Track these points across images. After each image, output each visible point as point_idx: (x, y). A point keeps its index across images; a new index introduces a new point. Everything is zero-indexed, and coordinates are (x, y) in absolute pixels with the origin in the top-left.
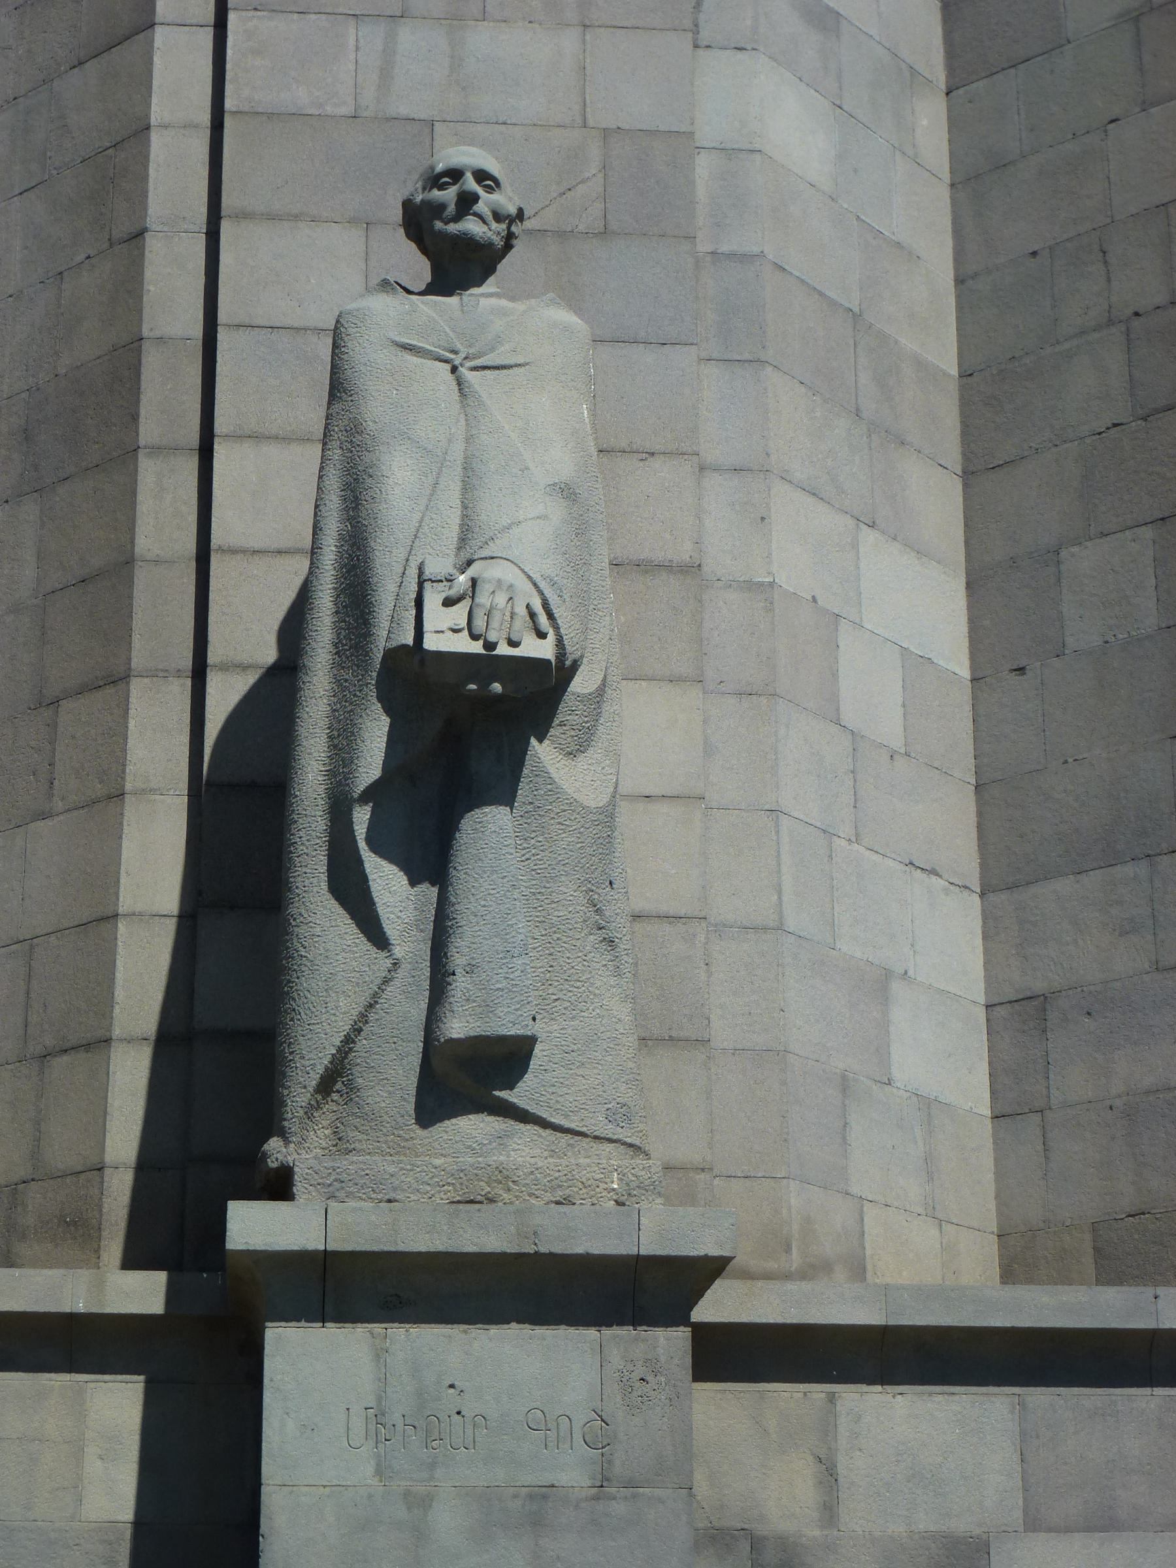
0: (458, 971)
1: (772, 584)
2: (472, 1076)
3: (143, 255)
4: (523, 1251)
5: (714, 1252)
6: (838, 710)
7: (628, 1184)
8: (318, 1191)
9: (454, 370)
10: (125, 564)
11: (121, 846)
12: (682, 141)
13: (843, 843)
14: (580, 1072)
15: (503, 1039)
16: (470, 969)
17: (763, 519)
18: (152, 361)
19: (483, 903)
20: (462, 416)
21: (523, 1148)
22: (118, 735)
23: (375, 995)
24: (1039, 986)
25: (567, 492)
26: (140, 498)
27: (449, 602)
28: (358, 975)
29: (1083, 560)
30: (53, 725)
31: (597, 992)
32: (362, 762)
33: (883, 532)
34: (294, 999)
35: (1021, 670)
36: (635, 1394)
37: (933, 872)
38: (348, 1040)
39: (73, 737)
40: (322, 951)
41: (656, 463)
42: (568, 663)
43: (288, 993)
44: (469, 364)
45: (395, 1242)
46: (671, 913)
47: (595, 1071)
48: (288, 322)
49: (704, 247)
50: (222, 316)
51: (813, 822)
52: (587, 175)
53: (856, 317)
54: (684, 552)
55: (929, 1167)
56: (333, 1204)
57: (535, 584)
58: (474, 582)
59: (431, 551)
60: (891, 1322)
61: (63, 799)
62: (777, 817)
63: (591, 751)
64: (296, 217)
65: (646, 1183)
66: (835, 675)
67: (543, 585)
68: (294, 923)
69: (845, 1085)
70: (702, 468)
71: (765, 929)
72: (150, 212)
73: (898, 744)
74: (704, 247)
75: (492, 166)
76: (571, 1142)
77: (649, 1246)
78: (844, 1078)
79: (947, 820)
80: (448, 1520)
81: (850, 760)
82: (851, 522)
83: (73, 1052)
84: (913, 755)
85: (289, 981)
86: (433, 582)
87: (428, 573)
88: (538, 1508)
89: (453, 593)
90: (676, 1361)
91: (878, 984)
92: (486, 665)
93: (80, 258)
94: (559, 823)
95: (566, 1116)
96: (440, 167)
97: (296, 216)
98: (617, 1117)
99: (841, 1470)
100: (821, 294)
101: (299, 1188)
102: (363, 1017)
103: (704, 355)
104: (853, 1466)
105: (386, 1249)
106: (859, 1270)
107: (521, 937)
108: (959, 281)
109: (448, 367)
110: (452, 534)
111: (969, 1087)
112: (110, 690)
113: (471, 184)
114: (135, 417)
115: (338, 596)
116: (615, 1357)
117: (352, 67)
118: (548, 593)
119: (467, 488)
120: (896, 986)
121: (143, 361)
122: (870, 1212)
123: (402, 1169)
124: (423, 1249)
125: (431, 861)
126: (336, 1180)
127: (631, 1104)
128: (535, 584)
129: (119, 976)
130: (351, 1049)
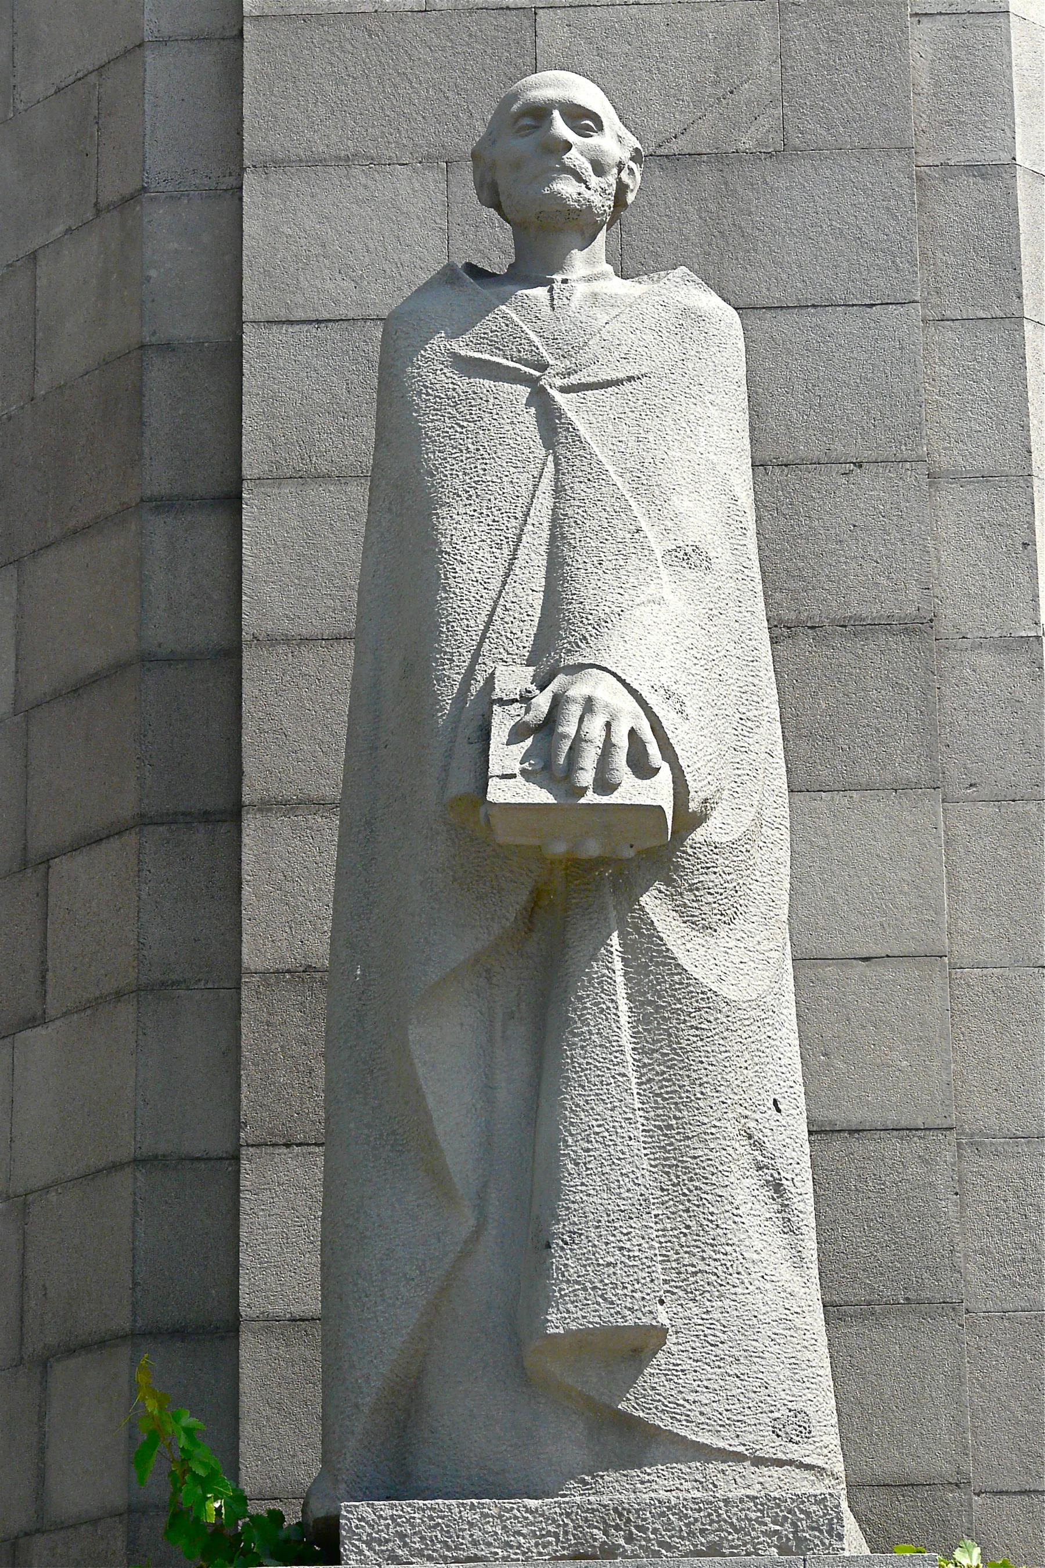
31: (755, 1257)
42: (693, 806)
46: (903, 1124)
59: (505, 656)
67: (652, 700)
75: (587, 94)
94: (692, 1027)
101: (346, 1548)
103: (931, 314)
110: (526, 633)
127: (810, 1411)
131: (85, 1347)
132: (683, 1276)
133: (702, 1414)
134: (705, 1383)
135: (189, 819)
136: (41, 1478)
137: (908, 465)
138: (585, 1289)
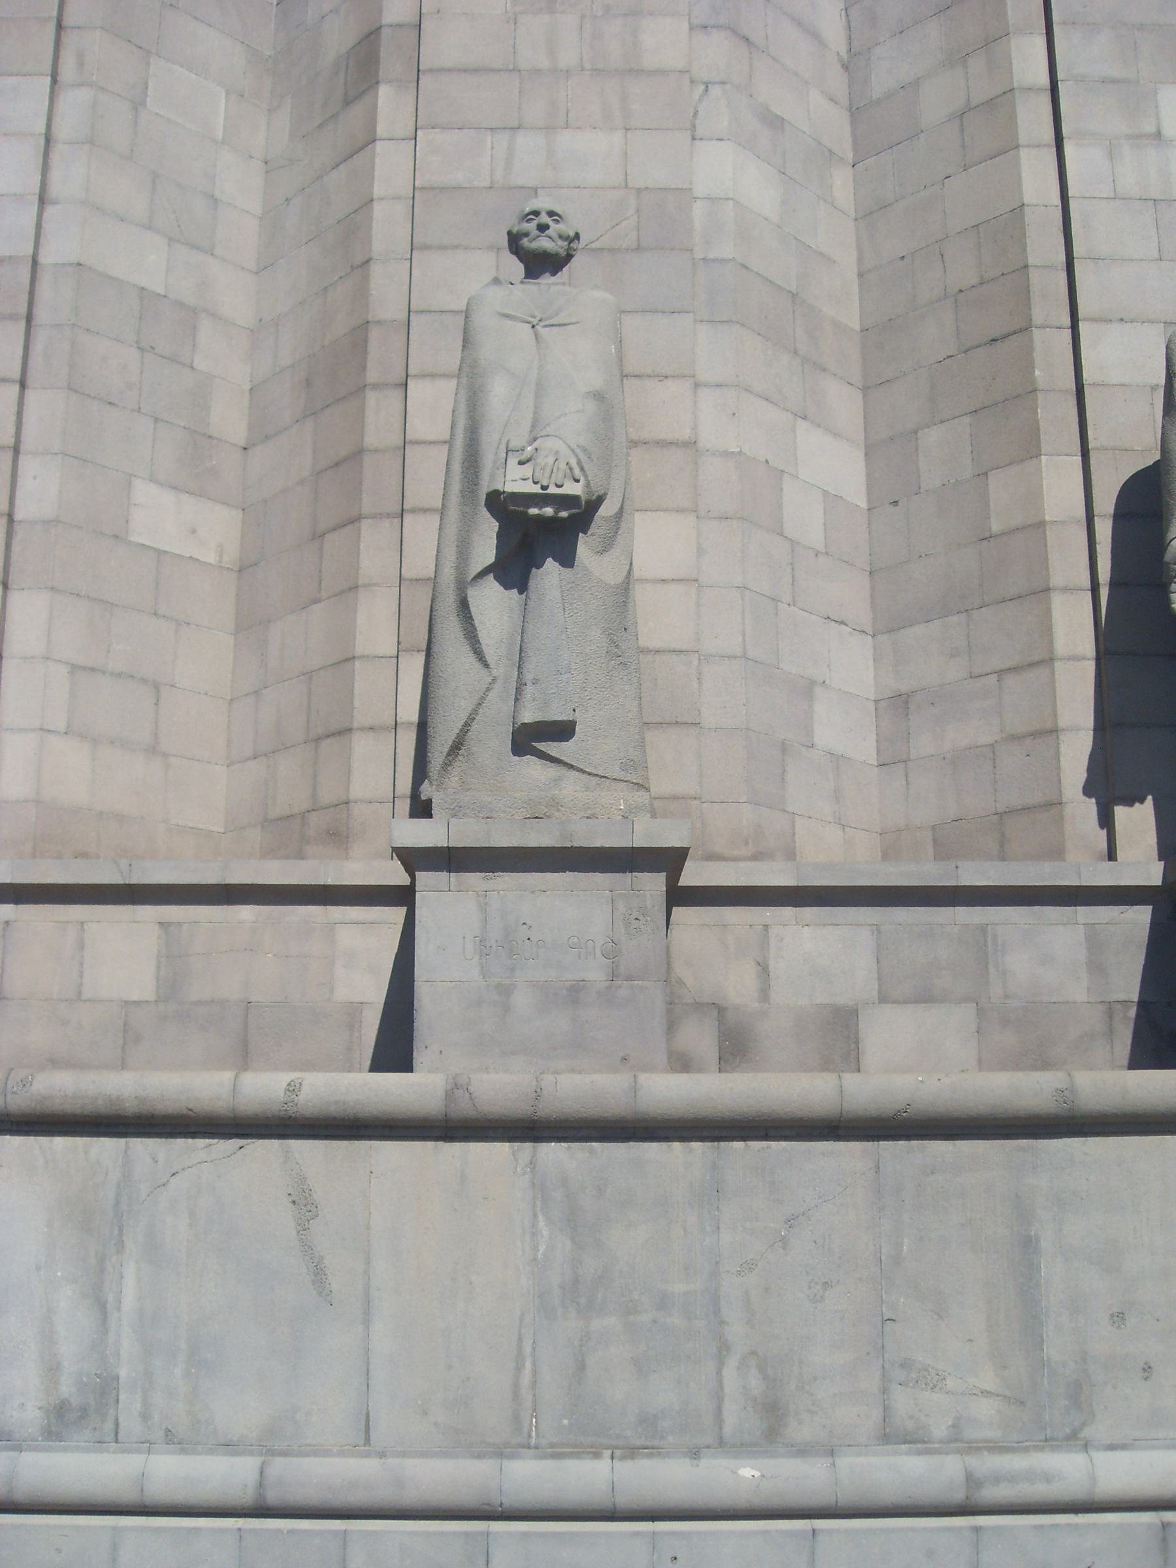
0: (529, 683)
12: (685, 193)
16: (535, 682)
18: (375, 335)
21: (571, 787)
24: (904, 689)
25: (598, 396)
27: (521, 463)
29: (932, 437)
35: (896, 503)
37: (843, 623)
38: (467, 724)
41: (669, 382)
44: (542, 324)
49: (699, 255)
54: (686, 434)
55: (837, 795)
56: (453, 821)
57: (573, 451)
64: (456, 247)
66: (780, 506)
67: (578, 451)
69: (784, 748)
70: (697, 385)
71: (735, 657)
74: (699, 255)
78: (783, 743)
79: (850, 593)
80: (522, 1000)
87: (510, 447)
88: (575, 993)
89: (524, 457)
91: (807, 689)
93: (337, 277)
96: (527, 210)
99: (771, 969)
102: (475, 711)
104: (778, 967)
106: (791, 854)
108: (860, 275)
111: (863, 747)
113: (544, 219)
116: (621, 907)
118: (582, 456)
119: (538, 396)
120: (818, 690)
122: (799, 822)
128: (573, 451)
131: (333, 734)
136: (314, 789)
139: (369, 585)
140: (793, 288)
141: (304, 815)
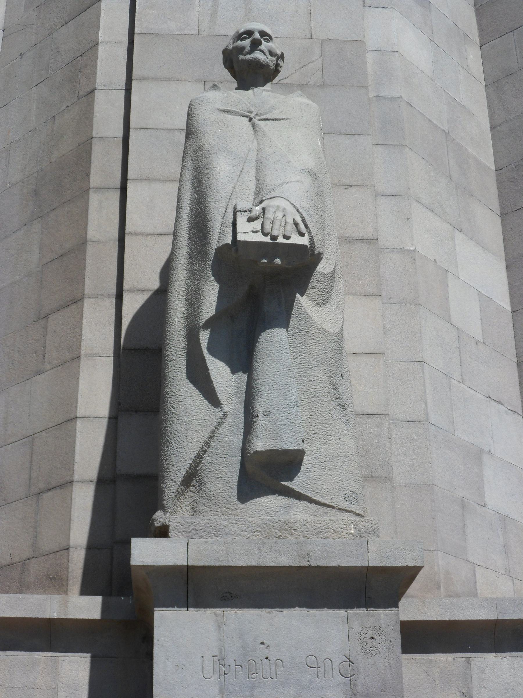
0: (260, 415)
1: (414, 250)
2: (269, 473)
3: (94, 100)
4: (302, 565)
5: (411, 564)
6: (450, 316)
7: (359, 531)
8: (182, 535)
9: (250, 120)
10: (82, 244)
11: (78, 382)
13: (456, 382)
14: (329, 473)
15: (286, 452)
16: (267, 414)
17: (408, 219)
18: (97, 149)
19: (273, 379)
20: (255, 140)
21: (299, 512)
22: (78, 327)
23: (213, 432)
25: (312, 174)
26: (90, 211)
27: (250, 220)
28: (204, 421)
30: (45, 328)
31: (337, 431)
32: (205, 307)
33: (466, 235)
34: (168, 436)
36: (368, 646)
37: (500, 402)
38: (199, 456)
39: (55, 332)
40: (184, 409)
41: (353, 190)
42: (316, 252)
43: (165, 433)
44: (258, 118)
45: (228, 561)
46: (370, 413)
47: (338, 473)
48: (165, 126)
50: (132, 124)
51: (441, 370)
52: (313, 59)
53: (447, 134)
54: (369, 232)
57: (297, 210)
58: (264, 209)
60: (500, 618)
61: (50, 363)
62: (423, 365)
63: (328, 305)
64: (169, 79)
65: (370, 530)
66: (447, 299)
67: (301, 210)
68: (168, 396)
69: (463, 504)
71: (419, 422)
72: (98, 80)
73: (480, 338)
76: (326, 511)
77: (375, 561)
78: (462, 501)
81: (457, 341)
82: (451, 228)
83: (53, 490)
84: (486, 344)
85: (166, 427)
86: (241, 212)
87: (238, 208)
89: (253, 214)
90: (391, 627)
92: (272, 248)
94: (313, 339)
95: (323, 497)
96: (242, 30)
97: (169, 79)
98: (351, 498)
100: (430, 121)
101: (172, 533)
102: (207, 444)
105: (222, 565)
107: (294, 397)
108: (492, 128)
109: (247, 119)
112: (74, 306)
113: (257, 36)
114: (88, 175)
115: (191, 230)
116: (356, 627)
117: (197, 13)
118: (304, 214)
119: (258, 171)
121: (93, 148)
122: (479, 572)
123: (231, 523)
124: (244, 564)
125: (243, 359)
126: (193, 529)
128: (297, 210)
129: (78, 448)
130: (200, 462)
132: (310, 434)
133: (317, 488)
134: (319, 477)
135: (102, 297)
137: (368, 187)
138: (273, 433)
139: (90, 355)
140: (446, 128)
141: (24, 563)
